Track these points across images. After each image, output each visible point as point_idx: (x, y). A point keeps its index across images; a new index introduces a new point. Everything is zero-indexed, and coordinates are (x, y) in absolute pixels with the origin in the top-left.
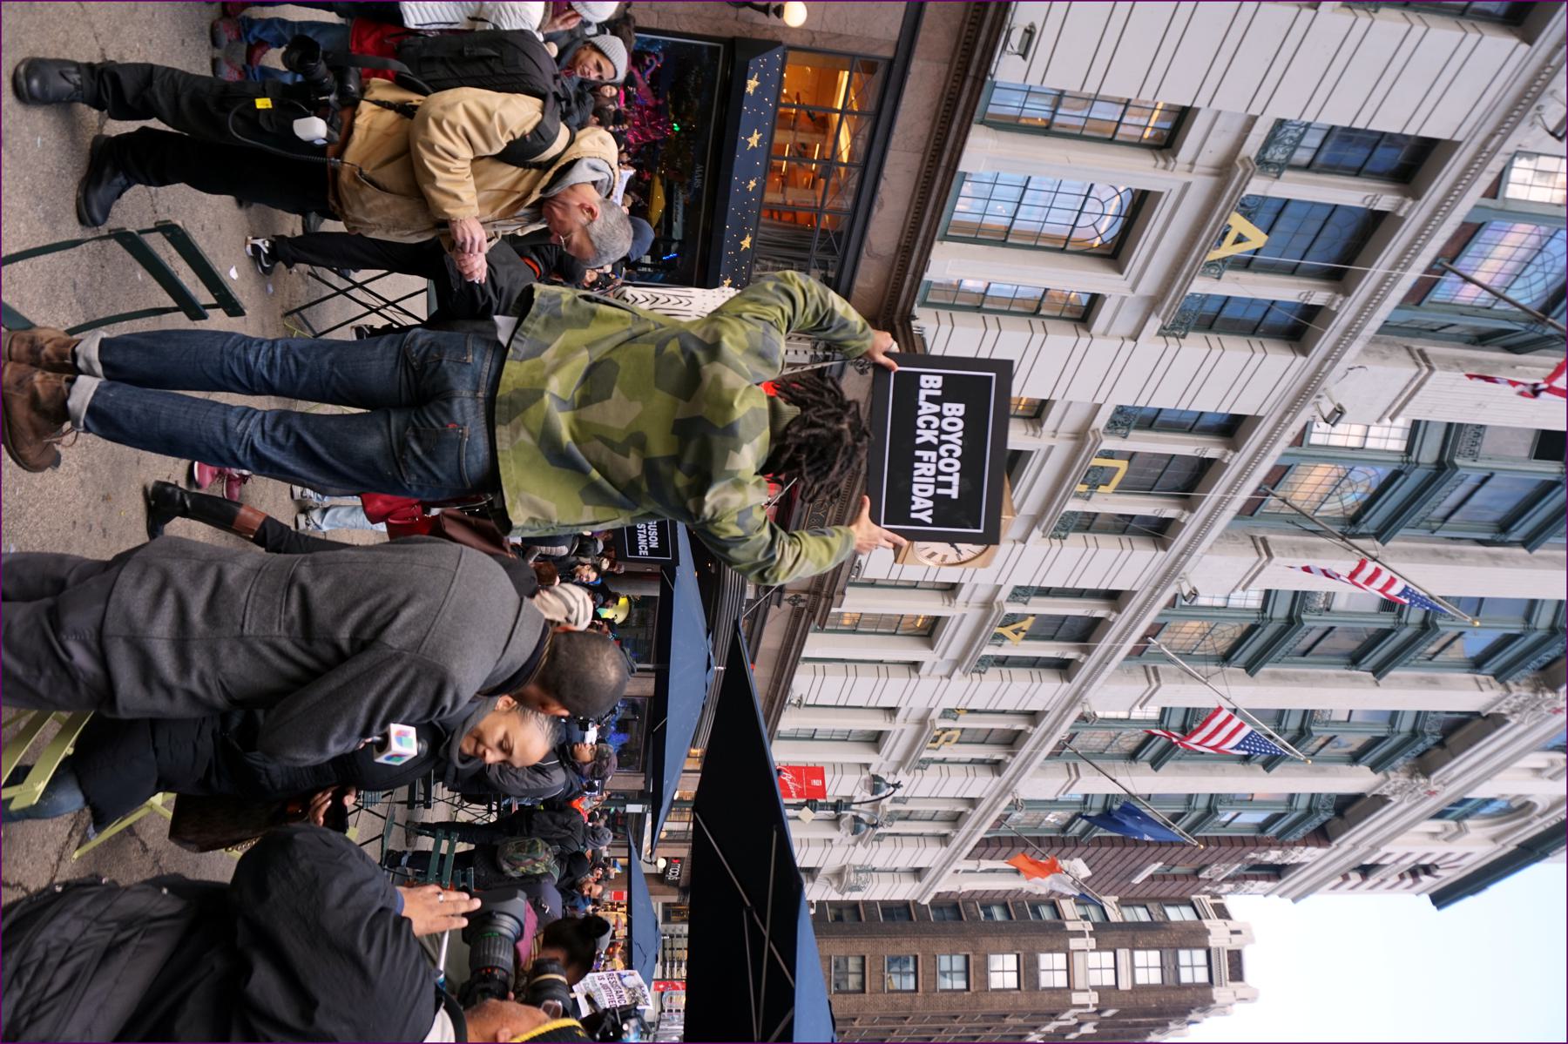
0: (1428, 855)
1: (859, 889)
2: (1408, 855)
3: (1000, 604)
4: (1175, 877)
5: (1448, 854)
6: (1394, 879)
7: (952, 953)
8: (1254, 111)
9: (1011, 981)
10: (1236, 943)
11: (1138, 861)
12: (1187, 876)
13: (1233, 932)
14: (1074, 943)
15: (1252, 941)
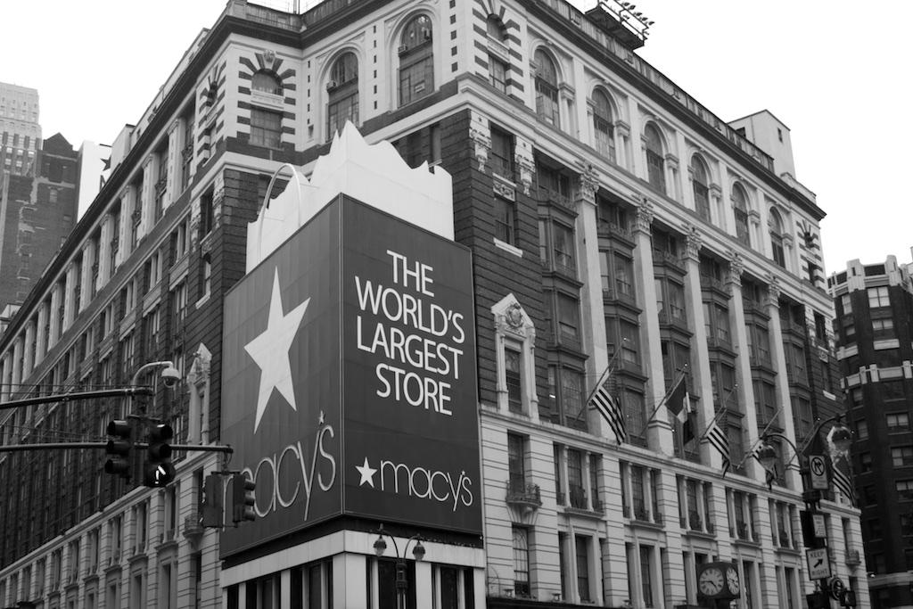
0: (801, 246)
1: (857, 553)
2: (802, 257)
3: (736, 541)
4: (829, 376)
5: (799, 235)
6: (816, 251)
7: (891, 458)
8: (622, 526)
9: (903, 420)
10: (860, 271)
11: (824, 404)
12: (829, 369)
13: (854, 274)
14: (875, 379)
15: (857, 261)
